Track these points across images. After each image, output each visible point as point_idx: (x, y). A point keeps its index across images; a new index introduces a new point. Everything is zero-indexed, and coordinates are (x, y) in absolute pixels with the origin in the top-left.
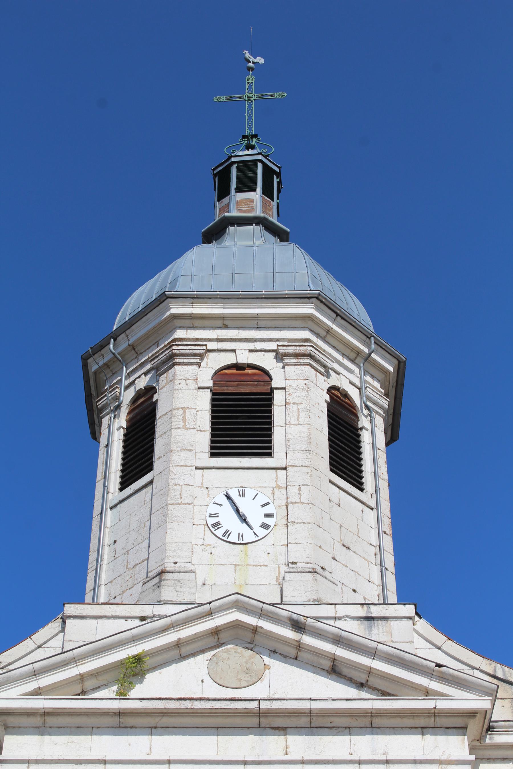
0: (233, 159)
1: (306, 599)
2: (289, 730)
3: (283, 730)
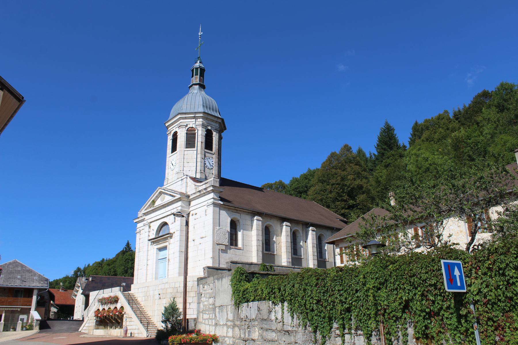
0: (194, 67)
3: (166, 207)
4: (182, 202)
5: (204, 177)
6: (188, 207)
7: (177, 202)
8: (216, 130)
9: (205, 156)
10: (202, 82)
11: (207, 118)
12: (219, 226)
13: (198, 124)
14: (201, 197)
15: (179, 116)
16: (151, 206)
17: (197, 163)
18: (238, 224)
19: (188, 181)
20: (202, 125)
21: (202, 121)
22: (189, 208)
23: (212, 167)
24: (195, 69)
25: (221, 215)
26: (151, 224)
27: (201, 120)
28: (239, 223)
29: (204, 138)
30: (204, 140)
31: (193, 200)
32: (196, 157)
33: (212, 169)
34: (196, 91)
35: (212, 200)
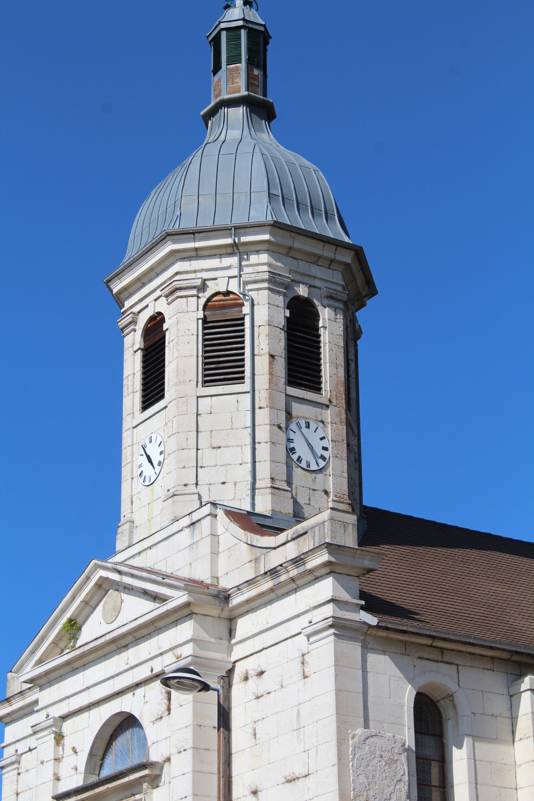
0: (223, 26)
1: (168, 522)
2: (129, 646)
3: (126, 647)
4: (196, 621)
5: (289, 509)
6: (226, 642)
7: (176, 623)
8: (330, 297)
9: (289, 414)
10: (260, 89)
11: (290, 248)
12: (366, 725)
13: (253, 277)
14: (280, 598)
15: (169, 247)
16: (62, 645)
17: (254, 449)
18: (448, 713)
19: (220, 530)
20: (269, 281)
21: (269, 265)
22: (230, 649)
23: (322, 464)
24: (224, 34)
25: (370, 676)
26: (67, 727)
27: (264, 258)
28: (455, 707)
29: (282, 335)
30: (282, 344)
31: (247, 612)
32: (249, 423)
33: (320, 470)
34: (234, 134)
35: (329, 610)
